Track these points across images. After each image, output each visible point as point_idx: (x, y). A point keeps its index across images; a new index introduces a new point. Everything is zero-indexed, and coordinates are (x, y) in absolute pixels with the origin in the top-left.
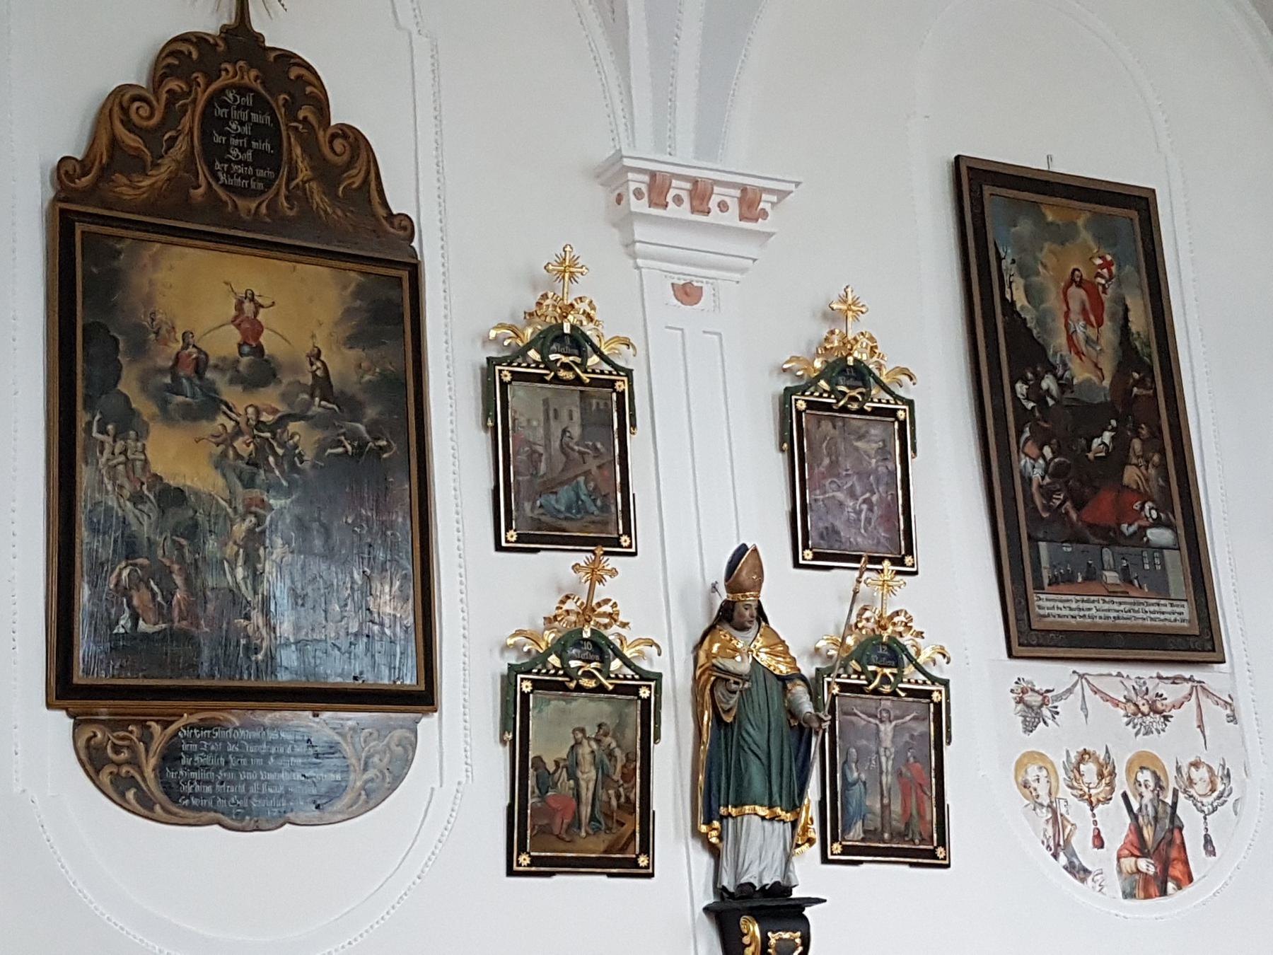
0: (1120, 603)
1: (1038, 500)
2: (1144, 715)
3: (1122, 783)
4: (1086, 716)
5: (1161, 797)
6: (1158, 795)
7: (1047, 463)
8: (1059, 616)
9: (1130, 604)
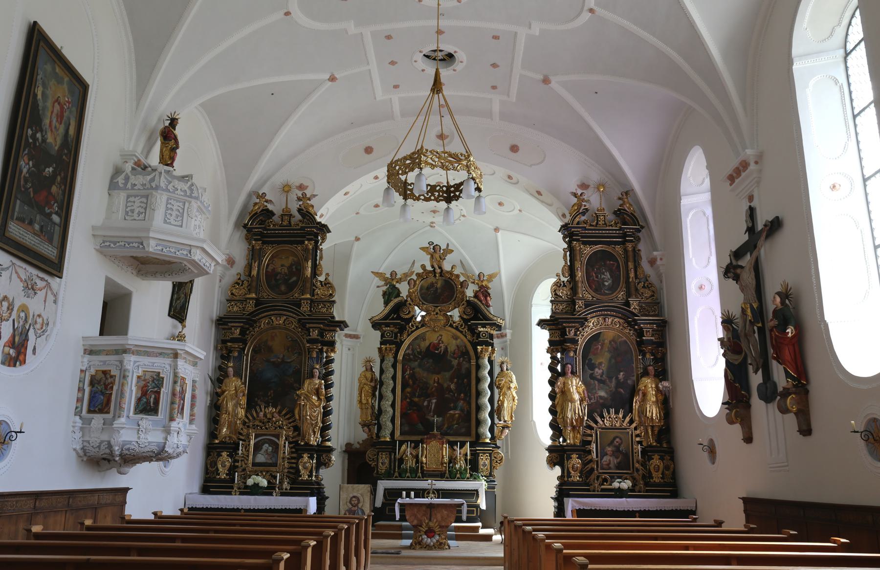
0: (37, 239)
1: (22, 182)
2: (29, 289)
3: (14, 315)
4: (10, 282)
6: (24, 324)
8: (15, 234)
9: (40, 241)
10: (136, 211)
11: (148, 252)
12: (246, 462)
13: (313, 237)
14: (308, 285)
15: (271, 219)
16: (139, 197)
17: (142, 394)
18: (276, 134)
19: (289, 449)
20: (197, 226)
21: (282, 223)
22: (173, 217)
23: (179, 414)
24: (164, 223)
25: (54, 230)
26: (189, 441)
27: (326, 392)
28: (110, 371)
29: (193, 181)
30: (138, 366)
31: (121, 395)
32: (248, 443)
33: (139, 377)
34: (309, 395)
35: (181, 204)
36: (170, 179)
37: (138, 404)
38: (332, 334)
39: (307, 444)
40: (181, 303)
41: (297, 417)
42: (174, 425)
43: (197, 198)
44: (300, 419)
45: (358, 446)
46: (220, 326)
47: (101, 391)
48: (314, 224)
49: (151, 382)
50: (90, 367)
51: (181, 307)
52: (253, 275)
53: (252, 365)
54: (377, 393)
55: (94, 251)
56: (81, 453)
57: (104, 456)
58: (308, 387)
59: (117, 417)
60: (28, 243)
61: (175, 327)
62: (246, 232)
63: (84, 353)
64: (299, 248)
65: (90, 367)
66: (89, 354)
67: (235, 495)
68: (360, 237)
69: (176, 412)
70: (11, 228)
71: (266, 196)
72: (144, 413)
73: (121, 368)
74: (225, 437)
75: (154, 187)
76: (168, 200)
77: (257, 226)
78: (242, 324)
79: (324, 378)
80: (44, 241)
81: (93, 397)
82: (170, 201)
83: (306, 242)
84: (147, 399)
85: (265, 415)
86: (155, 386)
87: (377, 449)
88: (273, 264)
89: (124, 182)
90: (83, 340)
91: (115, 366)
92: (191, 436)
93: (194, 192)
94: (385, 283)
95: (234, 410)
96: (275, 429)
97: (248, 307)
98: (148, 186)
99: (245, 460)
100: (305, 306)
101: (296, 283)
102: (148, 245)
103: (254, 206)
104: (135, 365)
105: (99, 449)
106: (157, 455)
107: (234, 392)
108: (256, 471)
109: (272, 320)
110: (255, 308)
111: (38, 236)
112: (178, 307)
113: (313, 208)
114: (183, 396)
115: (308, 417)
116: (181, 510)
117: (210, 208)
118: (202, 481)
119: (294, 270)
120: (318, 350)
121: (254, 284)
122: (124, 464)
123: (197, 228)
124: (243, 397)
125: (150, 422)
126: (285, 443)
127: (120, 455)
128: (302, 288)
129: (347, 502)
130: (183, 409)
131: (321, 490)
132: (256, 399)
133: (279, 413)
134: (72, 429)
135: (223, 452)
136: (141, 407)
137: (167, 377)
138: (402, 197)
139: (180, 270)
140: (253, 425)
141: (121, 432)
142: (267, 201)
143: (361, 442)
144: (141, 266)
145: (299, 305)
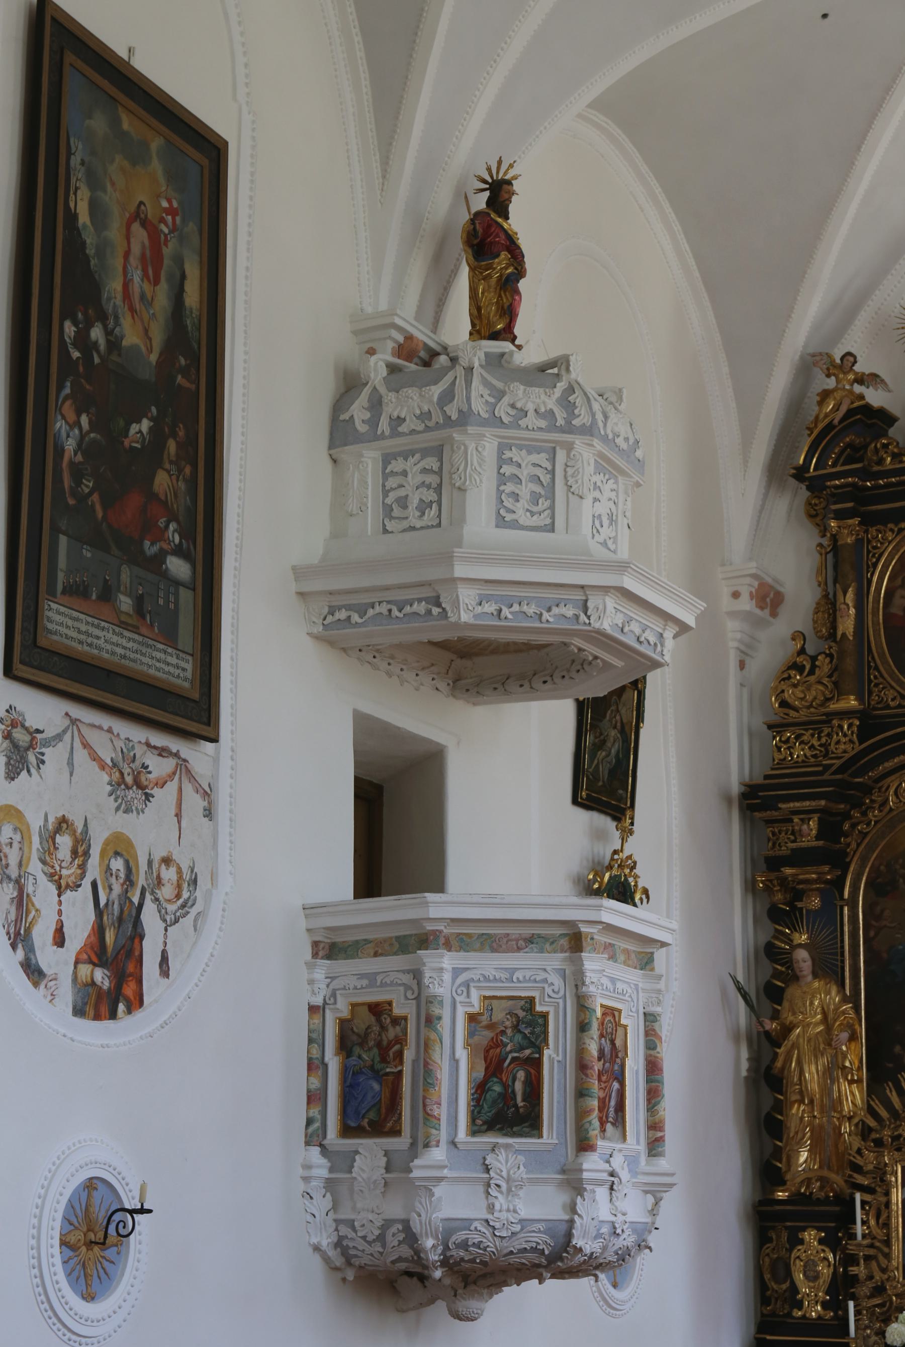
0: (129, 639)
1: (67, 481)
2: (128, 788)
3: (94, 870)
4: (71, 775)
5: (129, 894)
6: (127, 892)
7: (82, 436)
8: (67, 636)
9: (139, 643)
10: (414, 502)
11: (457, 625)
12: (883, 1262)
15: (885, 434)
16: (417, 456)
17: (487, 1069)
18: (859, 148)
22: (523, 504)
23: (609, 1127)
24: (497, 526)
25: (176, 603)
28: (390, 1003)
29: (573, 375)
30: (467, 985)
31: (425, 1079)
32: (883, 1199)
33: (472, 1018)
35: (542, 459)
36: (499, 385)
37: (478, 1100)
43: (588, 431)
46: (757, 814)
47: (372, 1067)
49: (509, 1031)
50: (334, 995)
51: (612, 772)
53: (872, 934)
55: (309, 641)
56: (339, 1261)
57: (402, 1266)
59: (420, 1145)
60: (106, 656)
61: (599, 835)
62: (809, 494)
63: (315, 955)
65: (334, 995)
66: (329, 957)
69: (596, 1123)
70: (50, 620)
71: (855, 362)
72: (500, 1130)
73: (419, 994)
74: (808, 1181)
75: (454, 417)
76: (500, 453)
77: (839, 469)
78: (823, 803)
80: (151, 642)
81: (351, 1086)
82: (508, 454)
84: (505, 1086)
89: (367, 415)
90: (306, 916)
91: (402, 988)
92: (658, 1195)
93: (576, 412)
95: (826, 1090)
97: (838, 742)
98: (437, 417)
99: (881, 1258)
102: (456, 603)
103: (821, 403)
104: (460, 980)
105: (384, 1246)
107: (821, 1028)
110: (860, 743)
111: (135, 629)
112: (604, 772)
114: (616, 1067)
117: (639, 453)
118: (752, 1330)
121: (850, 664)
122: (465, 1287)
123: (606, 522)
125: (521, 1158)
127: (445, 1262)
130: (620, 1107)
134: (302, 1187)
135: (804, 1229)
136: (488, 1112)
141: (438, 1191)
142: (860, 380)
144: (458, 663)
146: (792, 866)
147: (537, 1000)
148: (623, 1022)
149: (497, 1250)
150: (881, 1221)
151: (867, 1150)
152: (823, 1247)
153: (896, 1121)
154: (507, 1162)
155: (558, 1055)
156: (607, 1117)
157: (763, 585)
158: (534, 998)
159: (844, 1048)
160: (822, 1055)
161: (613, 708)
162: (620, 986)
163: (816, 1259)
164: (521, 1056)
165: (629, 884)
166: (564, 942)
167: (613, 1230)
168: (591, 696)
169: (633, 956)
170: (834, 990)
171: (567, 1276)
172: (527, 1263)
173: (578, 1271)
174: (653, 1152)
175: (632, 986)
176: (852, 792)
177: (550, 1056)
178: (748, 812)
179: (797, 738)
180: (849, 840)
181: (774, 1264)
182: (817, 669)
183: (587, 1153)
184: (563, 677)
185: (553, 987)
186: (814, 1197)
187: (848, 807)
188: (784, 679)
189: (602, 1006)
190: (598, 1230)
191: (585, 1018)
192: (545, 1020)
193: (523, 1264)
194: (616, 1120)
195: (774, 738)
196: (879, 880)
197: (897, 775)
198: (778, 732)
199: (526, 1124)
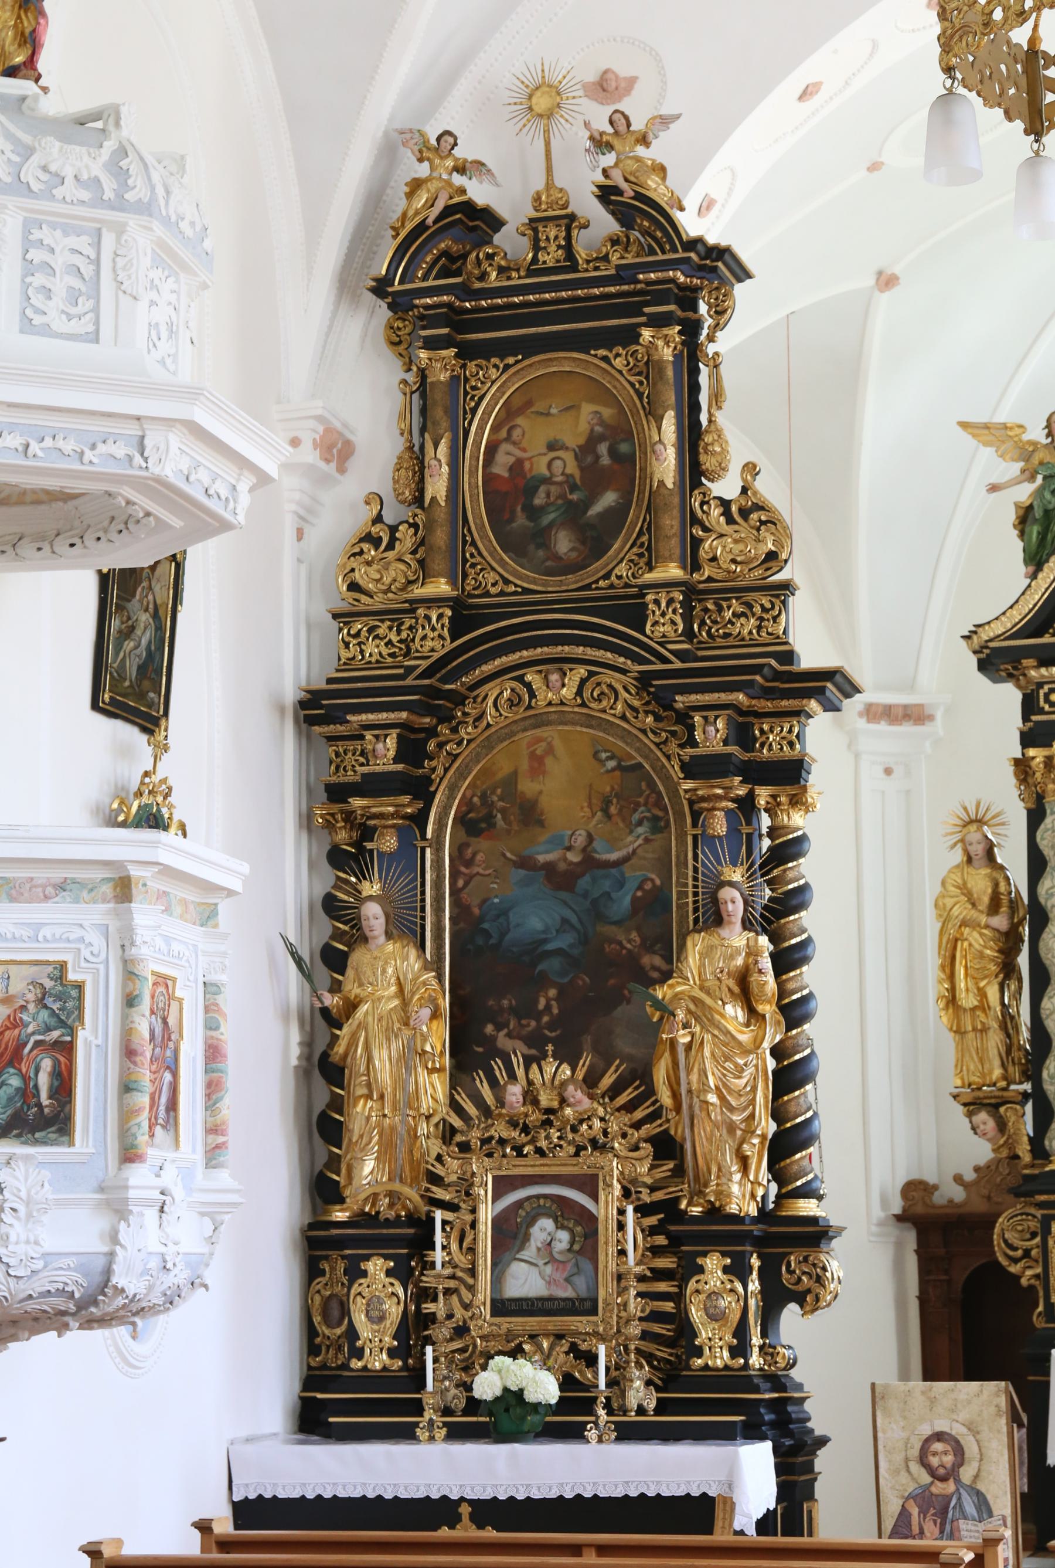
12: (467, 1296)
13: (672, 307)
14: (670, 522)
15: (489, 242)
19: (640, 1236)
20: (163, 329)
21: (535, 260)
22: (58, 302)
23: (158, 1130)
24: (22, 331)
26: (211, 1241)
27: (780, 985)
29: (125, 133)
32: (469, 1218)
34: (708, 1001)
35: (83, 243)
36: (26, 138)
38: (790, 731)
39: (715, 1213)
40: (142, 651)
41: (665, 1098)
42: (138, 1176)
43: (145, 208)
44: (678, 1108)
45: (958, 1194)
46: (317, 729)
48: (675, 251)
49: (31, 1007)
51: (140, 668)
52: (434, 499)
53: (460, 883)
54: (1023, 960)
58: (701, 967)
61: (125, 752)
62: (390, 314)
64: (618, 363)
67: (432, 1438)
68: (897, 270)
69: (145, 1125)
71: (456, 144)
76: (27, 232)
77: (430, 283)
78: (404, 715)
79: (770, 922)
82: (37, 234)
83: (646, 334)
84: (25, 1079)
85: (530, 1097)
86: (53, 1022)
87: (1040, 1205)
88: (514, 443)
92: (218, 1218)
93: (130, 182)
94: (1023, 471)
95: (400, 1083)
96: (577, 1154)
99: (464, 1291)
100: (663, 615)
101: (617, 516)
103: (410, 195)
106: (83, 1305)
108: (509, 1336)
109: (528, 686)
110: (452, 641)
112: (132, 670)
113: (664, 178)
114: (168, 1053)
115: (712, 1098)
116: (204, 1527)
117: (207, 244)
118: (297, 1386)
119: (606, 461)
120: (731, 805)
121: (440, 537)
123: (164, 334)
124: (435, 1023)
125: (46, 1174)
126: (621, 1212)
128: (645, 538)
129: (907, 1460)
130: (173, 1105)
131: (790, 1409)
132: (489, 1029)
133: (590, 1082)
135: (367, 1258)
137: (96, 982)
138: (1019, 125)
139: (113, 518)
140: (485, 1141)
142: (461, 169)
143: (970, 1176)
145: (637, 616)
146: (362, 795)
147: (70, 966)
148: (178, 993)
149: (11, 1294)
150: (464, 1246)
151: (449, 1156)
152: (392, 1280)
153: (486, 1118)
154: (26, 1180)
155: (96, 1038)
156: (156, 1118)
157: (329, 430)
158: (65, 962)
159: (425, 1028)
160: (396, 1036)
161: (145, 584)
162: (176, 947)
163: (382, 1295)
164: (47, 1039)
165: (162, 816)
166: (107, 889)
167: (163, 1264)
168: (118, 568)
169: (191, 907)
170: (413, 953)
171: (95, 1325)
172: (49, 1310)
173: (112, 1319)
174: (214, 1162)
175: (191, 947)
176: (441, 702)
177: (86, 1039)
178: (304, 726)
179: (370, 630)
180: (434, 763)
181: (326, 1302)
182: (397, 543)
183: (133, 1165)
184: (99, 539)
185: (91, 949)
186: (382, 1217)
187: (435, 721)
188: (354, 555)
189: (153, 973)
190: (145, 1265)
191: (134, 990)
192: (80, 992)
193: (45, 1311)
194: (167, 1122)
195: (341, 630)
196: (470, 815)
197: (498, 680)
198: (345, 623)
199: (53, 1129)
